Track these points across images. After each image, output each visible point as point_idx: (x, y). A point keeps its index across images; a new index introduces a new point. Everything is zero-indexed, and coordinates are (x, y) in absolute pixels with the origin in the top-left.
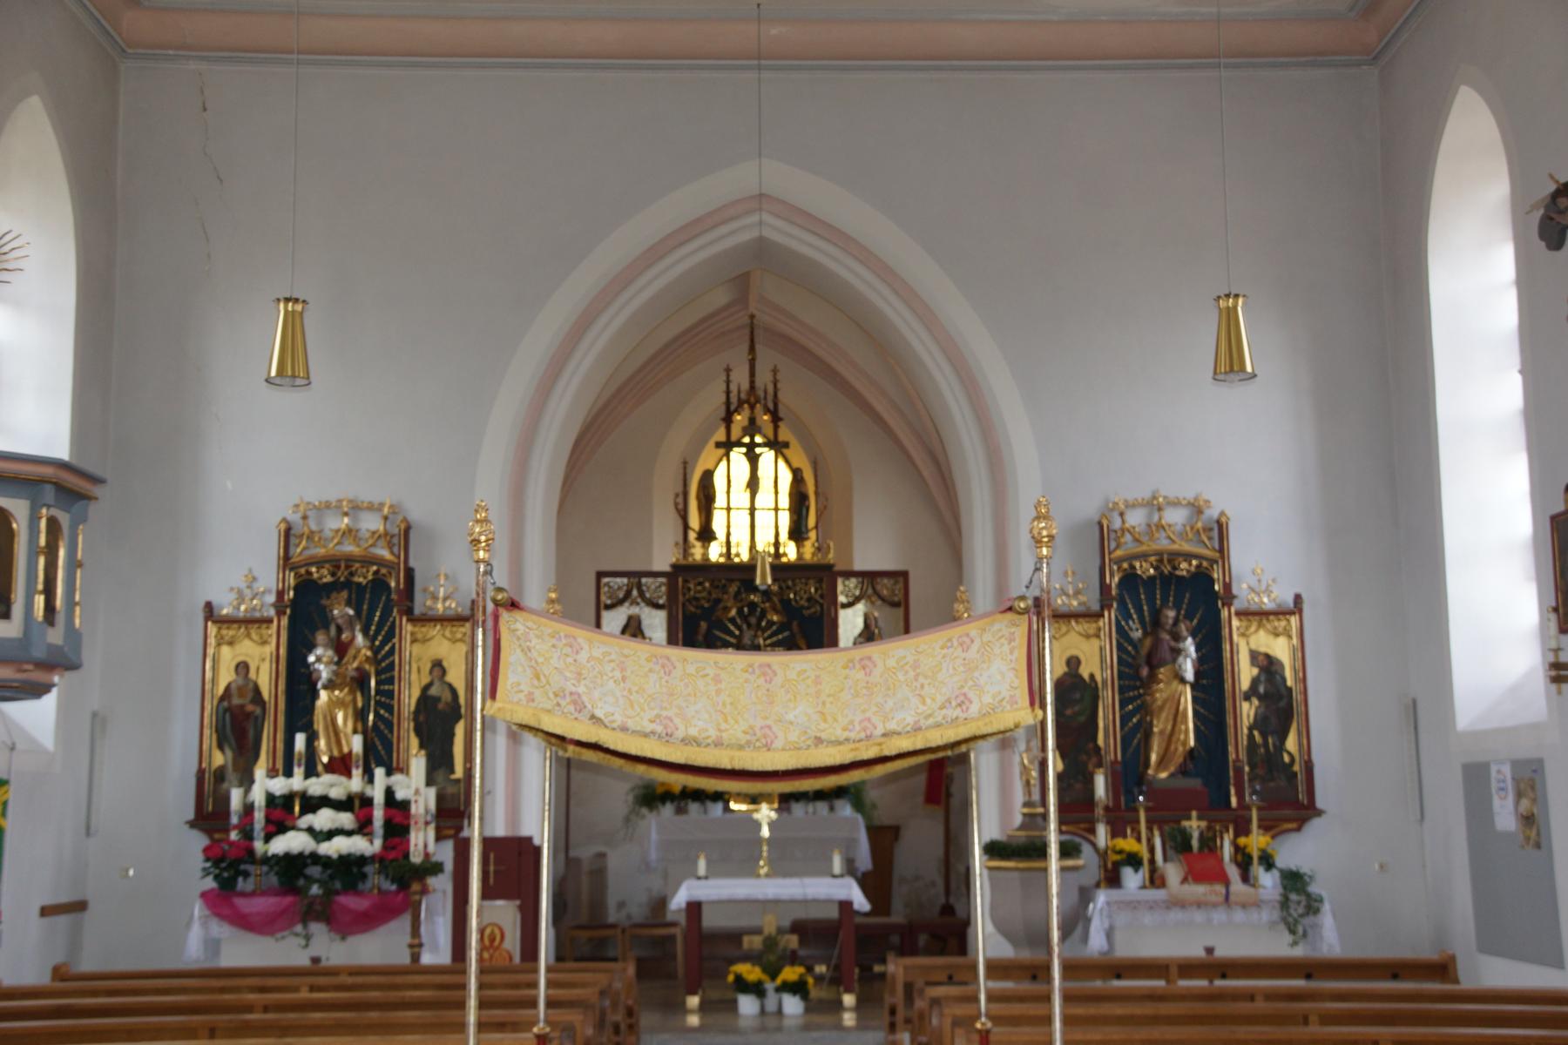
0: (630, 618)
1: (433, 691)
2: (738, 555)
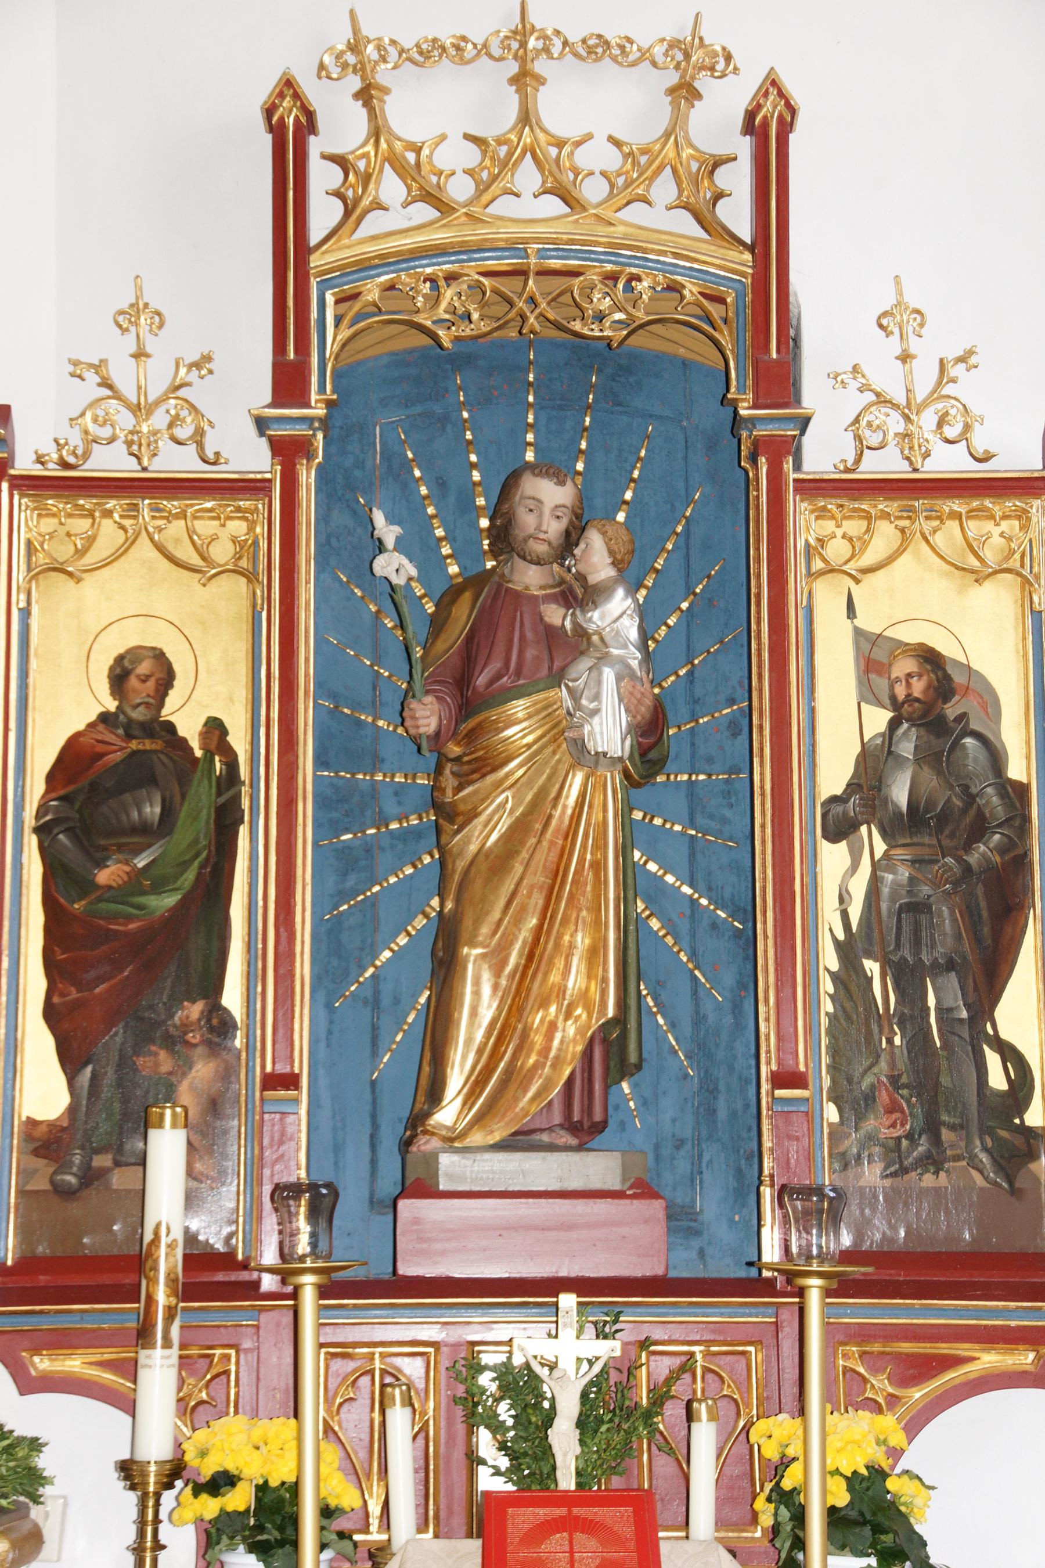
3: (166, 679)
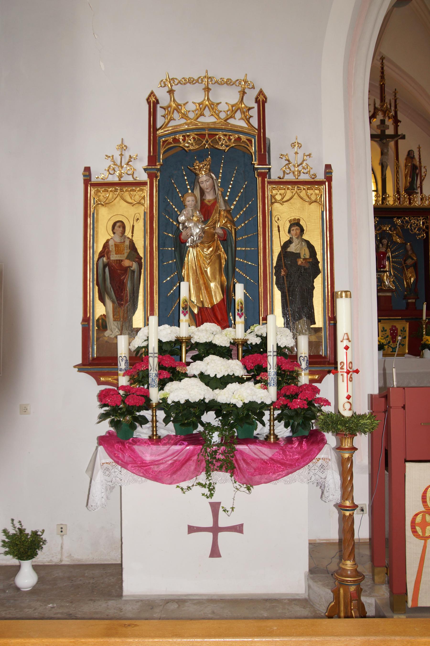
1: (292, 248)
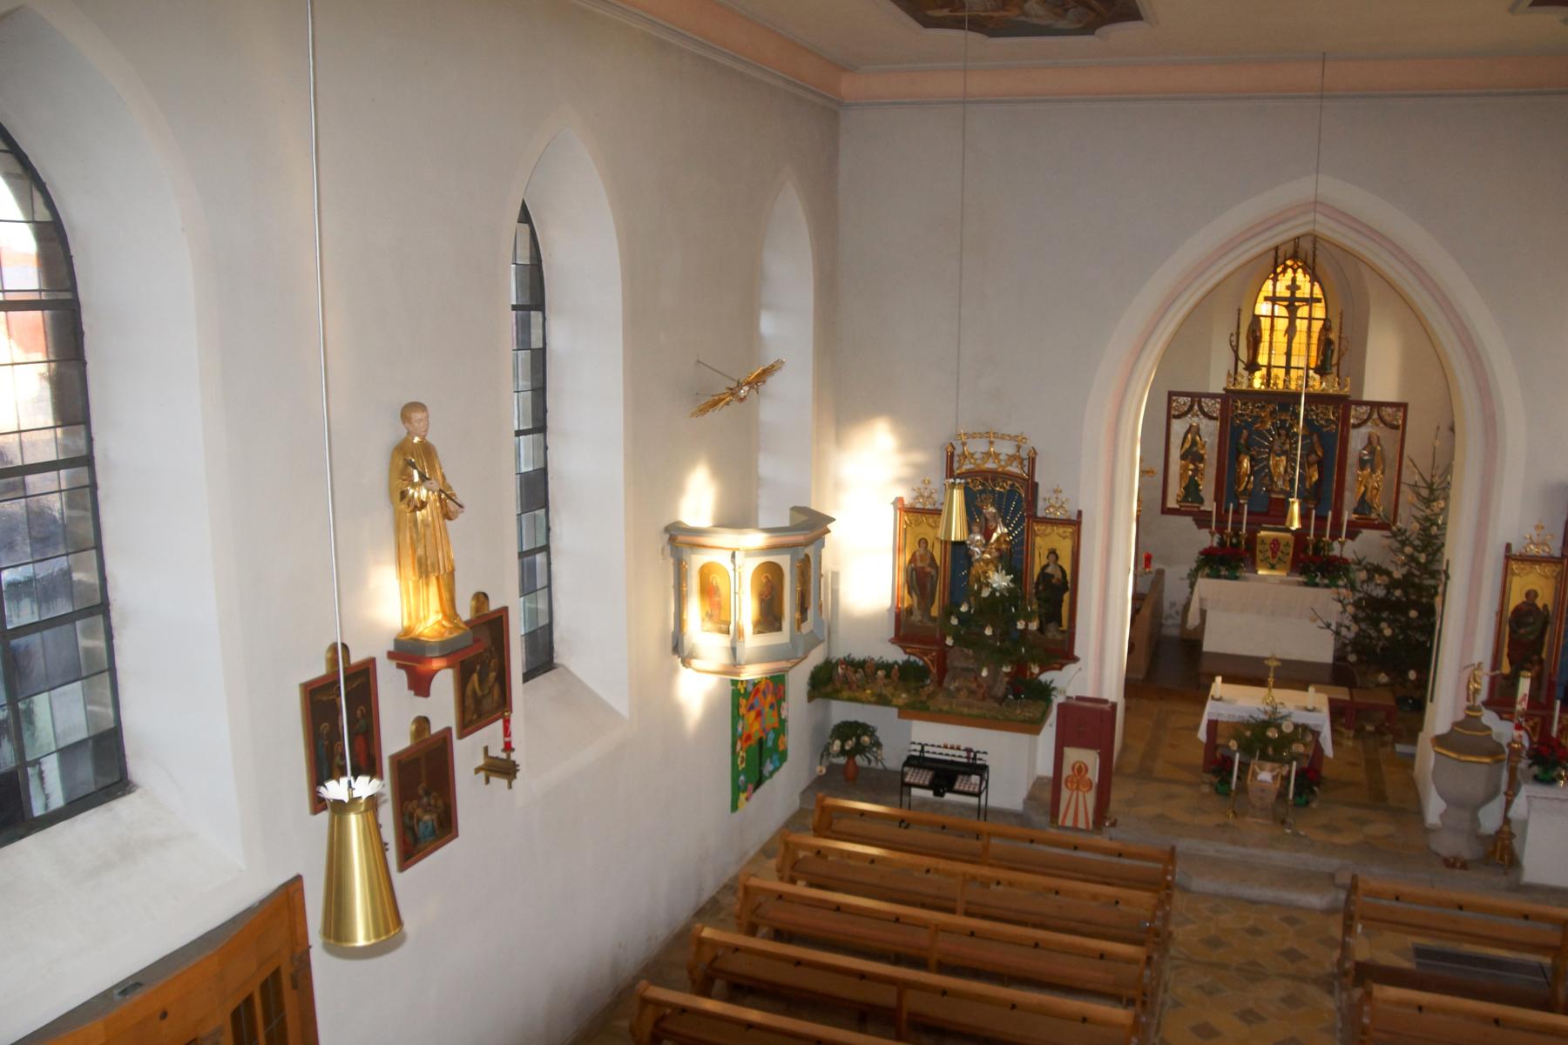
0: (1191, 426)
1: (1049, 570)
2: (1275, 384)
3: (1536, 595)
